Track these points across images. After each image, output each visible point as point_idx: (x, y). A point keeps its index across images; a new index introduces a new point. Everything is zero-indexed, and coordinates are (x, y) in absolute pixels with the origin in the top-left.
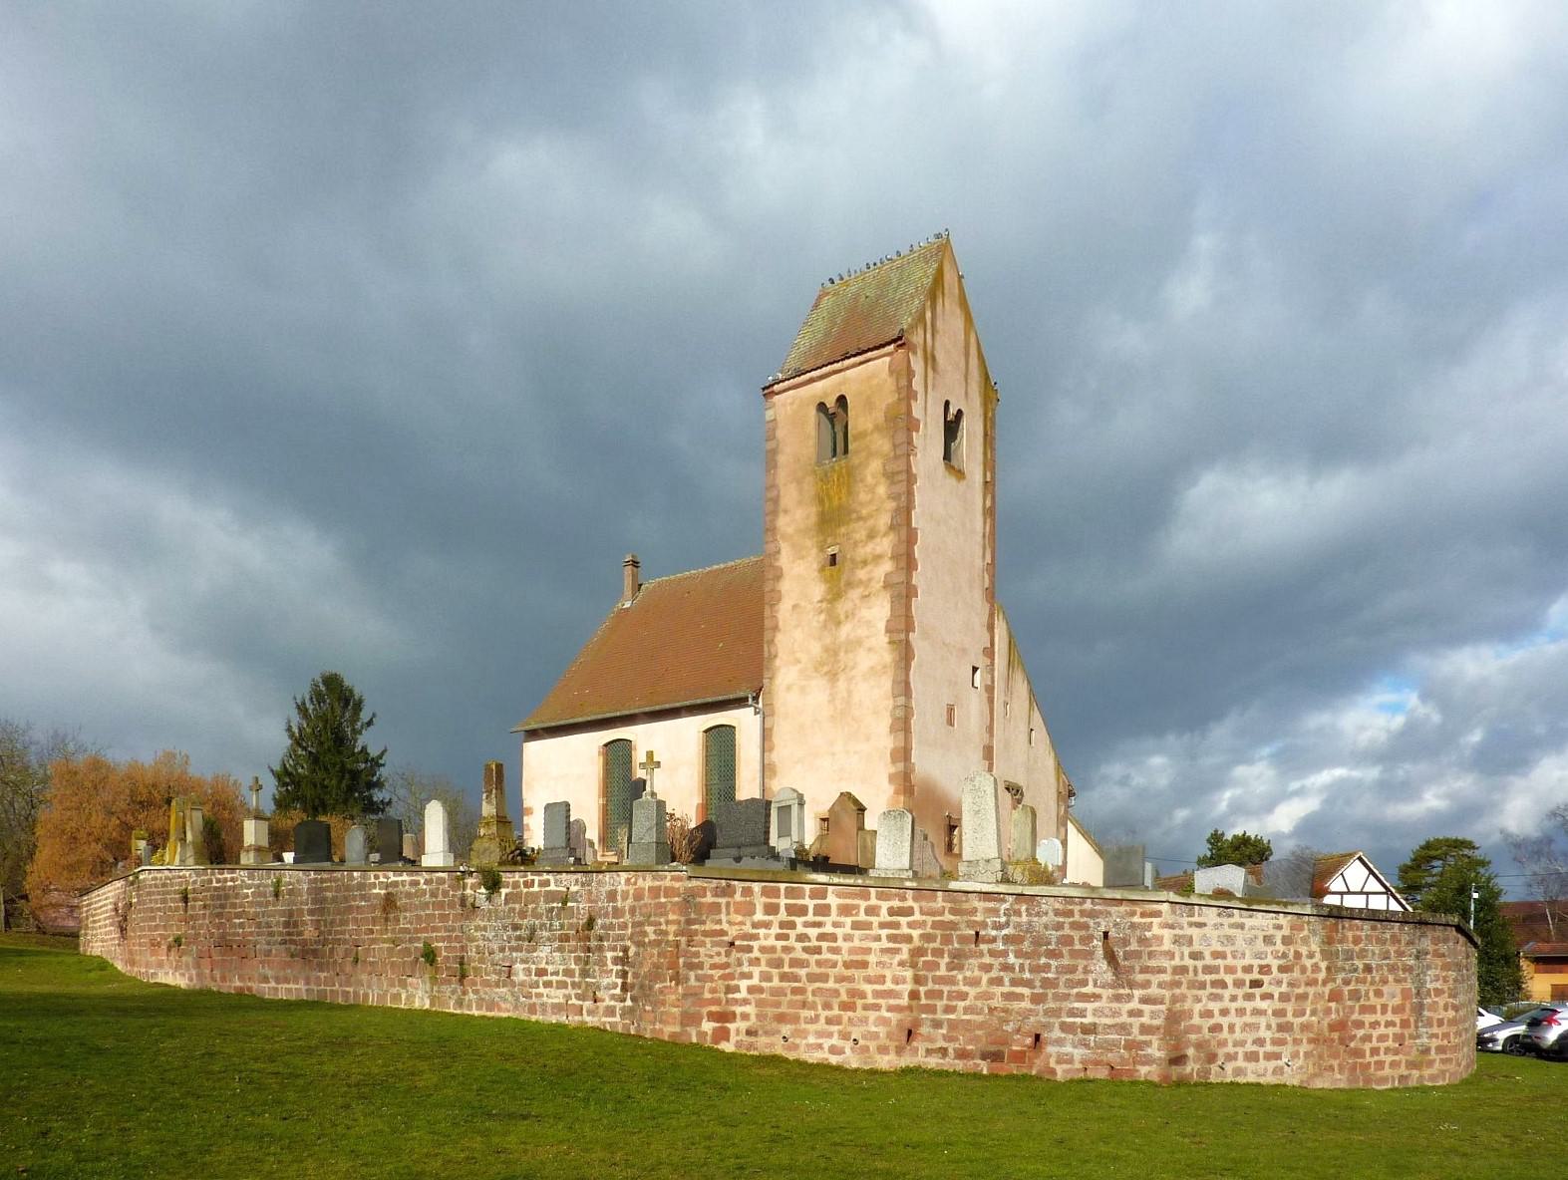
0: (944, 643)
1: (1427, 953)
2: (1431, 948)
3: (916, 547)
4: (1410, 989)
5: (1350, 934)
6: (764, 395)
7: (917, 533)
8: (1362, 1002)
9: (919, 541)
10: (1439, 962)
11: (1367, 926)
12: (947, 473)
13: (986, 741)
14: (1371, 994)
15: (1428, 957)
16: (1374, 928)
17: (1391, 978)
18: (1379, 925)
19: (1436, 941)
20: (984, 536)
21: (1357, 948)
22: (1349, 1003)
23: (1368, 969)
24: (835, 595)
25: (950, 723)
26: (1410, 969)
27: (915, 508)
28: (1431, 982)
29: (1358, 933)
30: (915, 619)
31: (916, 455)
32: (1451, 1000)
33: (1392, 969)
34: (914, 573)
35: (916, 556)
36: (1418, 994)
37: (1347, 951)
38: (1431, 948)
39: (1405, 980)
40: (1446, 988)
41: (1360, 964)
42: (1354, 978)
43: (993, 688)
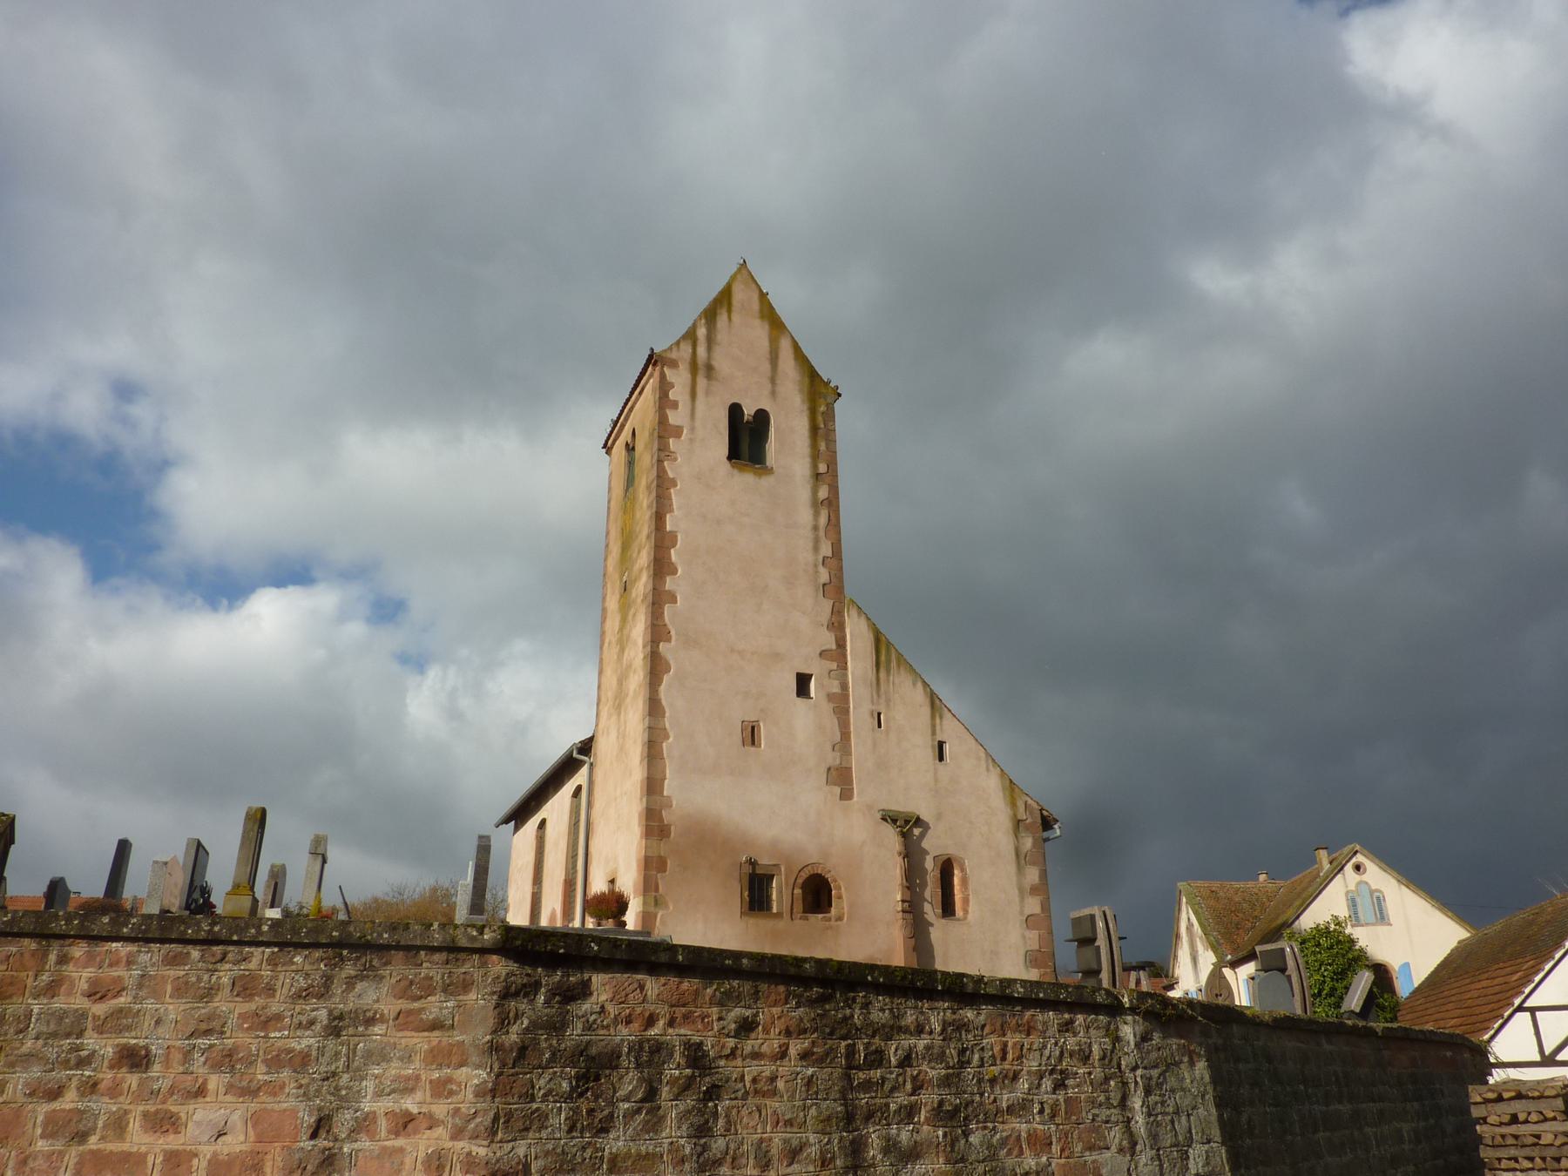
0: (732, 651)
1: (370, 1021)
2: (390, 1007)
3: (672, 551)
4: (294, 1112)
5: (82, 976)
6: (606, 453)
7: (676, 536)
8: (93, 1142)
9: (679, 543)
10: (421, 1042)
11: (148, 957)
12: (736, 471)
13: (833, 759)
14: (134, 1125)
15: (378, 1029)
16: (173, 961)
17: (215, 1082)
18: (195, 953)
19: (405, 990)
20: (816, 528)
21: (100, 1009)
22: (42, 1145)
23: (135, 1059)
24: (624, 620)
25: (941, 758)
26: (302, 1061)
27: (671, 511)
28: (379, 1094)
29: (116, 972)
30: (670, 627)
31: (676, 459)
32: (462, 1145)
33: (227, 1060)
34: (668, 579)
35: (674, 558)
36: (321, 1126)
37: (61, 1016)
38: (390, 1007)
39: (275, 1089)
40: (440, 1109)
41: (104, 1046)
42: (75, 1083)
43: (848, 696)
